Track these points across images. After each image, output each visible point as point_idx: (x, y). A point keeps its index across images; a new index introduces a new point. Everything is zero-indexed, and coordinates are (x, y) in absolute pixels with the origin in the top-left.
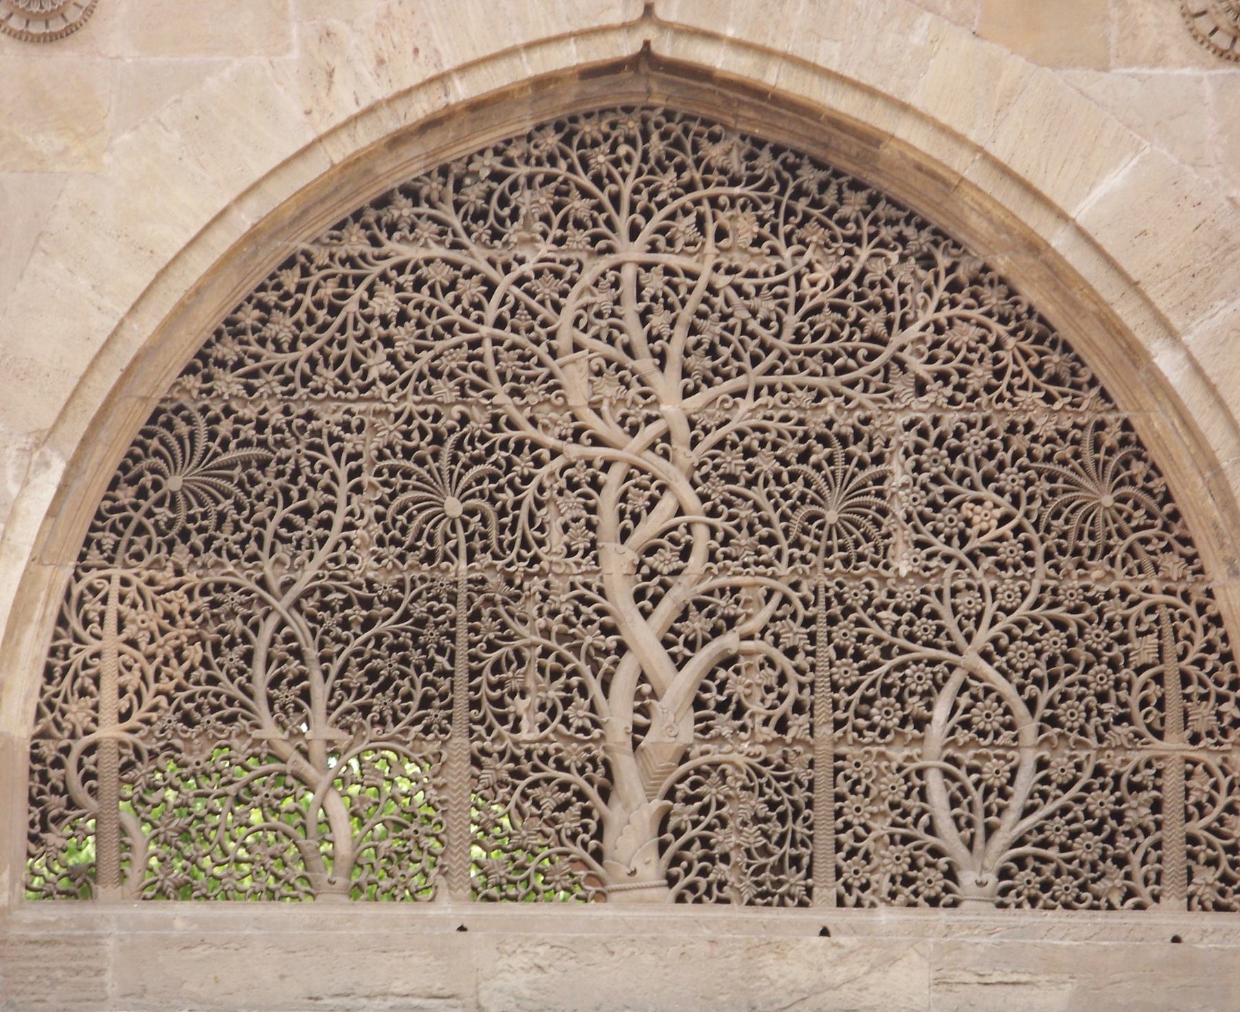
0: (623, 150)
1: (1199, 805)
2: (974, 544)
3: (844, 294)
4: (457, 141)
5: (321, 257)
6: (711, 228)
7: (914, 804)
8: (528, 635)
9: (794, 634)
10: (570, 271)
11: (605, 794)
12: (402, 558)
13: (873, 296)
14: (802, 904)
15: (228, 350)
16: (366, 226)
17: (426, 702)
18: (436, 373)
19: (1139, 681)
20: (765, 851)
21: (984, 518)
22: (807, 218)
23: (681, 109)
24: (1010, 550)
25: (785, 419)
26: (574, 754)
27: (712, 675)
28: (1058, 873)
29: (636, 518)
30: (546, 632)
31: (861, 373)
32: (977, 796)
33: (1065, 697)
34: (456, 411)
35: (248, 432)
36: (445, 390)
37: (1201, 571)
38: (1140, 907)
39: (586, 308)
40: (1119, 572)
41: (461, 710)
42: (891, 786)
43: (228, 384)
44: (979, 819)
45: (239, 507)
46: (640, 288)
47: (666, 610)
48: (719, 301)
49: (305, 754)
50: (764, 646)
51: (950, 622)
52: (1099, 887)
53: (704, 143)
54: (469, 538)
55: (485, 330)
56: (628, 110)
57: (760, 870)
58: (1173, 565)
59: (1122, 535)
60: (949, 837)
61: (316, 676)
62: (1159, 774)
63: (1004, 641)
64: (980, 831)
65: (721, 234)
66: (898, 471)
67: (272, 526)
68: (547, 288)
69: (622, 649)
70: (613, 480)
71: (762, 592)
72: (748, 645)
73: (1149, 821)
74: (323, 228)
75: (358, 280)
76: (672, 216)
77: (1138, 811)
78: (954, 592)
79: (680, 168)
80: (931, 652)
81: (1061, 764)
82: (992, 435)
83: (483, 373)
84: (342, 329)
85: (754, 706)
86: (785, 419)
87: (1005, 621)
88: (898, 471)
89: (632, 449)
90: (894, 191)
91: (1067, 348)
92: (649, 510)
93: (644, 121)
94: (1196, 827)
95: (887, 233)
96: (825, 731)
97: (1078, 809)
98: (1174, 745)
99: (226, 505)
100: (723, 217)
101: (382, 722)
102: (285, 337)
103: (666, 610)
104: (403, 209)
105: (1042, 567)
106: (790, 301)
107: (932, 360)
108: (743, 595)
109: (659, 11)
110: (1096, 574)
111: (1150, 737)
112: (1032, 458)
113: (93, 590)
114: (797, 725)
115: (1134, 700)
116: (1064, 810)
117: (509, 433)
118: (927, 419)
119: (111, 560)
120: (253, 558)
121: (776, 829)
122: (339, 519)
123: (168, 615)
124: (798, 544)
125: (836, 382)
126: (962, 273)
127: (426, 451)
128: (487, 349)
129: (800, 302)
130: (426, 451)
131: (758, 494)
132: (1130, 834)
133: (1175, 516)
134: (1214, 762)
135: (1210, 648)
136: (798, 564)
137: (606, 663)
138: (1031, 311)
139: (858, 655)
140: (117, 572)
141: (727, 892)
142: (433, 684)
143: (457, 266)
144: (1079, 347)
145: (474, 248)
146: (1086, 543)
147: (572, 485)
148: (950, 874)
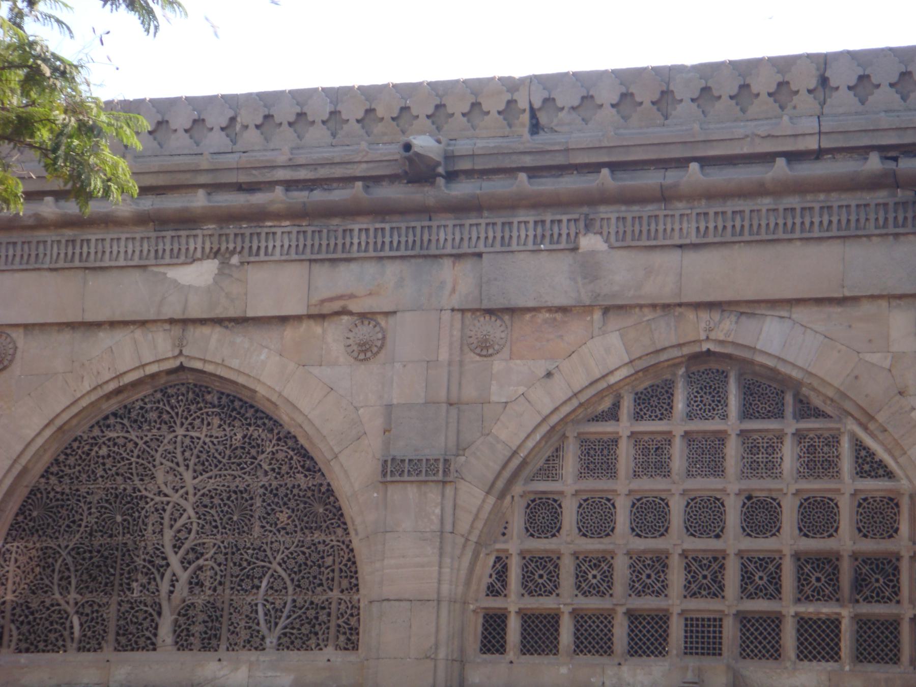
0: (180, 398)
1: (342, 614)
2: (279, 526)
3: (244, 443)
4: (128, 397)
5: (85, 437)
6: (205, 422)
7: (253, 615)
8: (139, 561)
9: (220, 558)
10: (161, 438)
11: (160, 614)
12: (102, 536)
13: (253, 443)
14: (216, 650)
15: (55, 469)
16: (100, 427)
17: (106, 584)
18: (117, 474)
19: (326, 572)
20: (206, 633)
21: (283, 517)
22: (235, 418)
23: (199, 383)
24: (290, 528)
25: (224, 486)
26: (149, 601)
27: (195, 573)
28: (296, 638)
29: (175, 520)
30: (144, 560)
31: (248, 469)
32: (272, 612)
33: (303, 578)
34: (122, 487)
35: (59, 496)
36: (119, 479)
37: (348, 534)
38: (321, 649)
39: (165, 450)
40: (323, 535)
41: (116, 587)
42: (246, 609)
43: (53, 480)
44: (273, 620)
45: (54, 521)
46: (183, 443)
47: (182, 552)
48: (206, 447)
49: (68, 603)
50: (211, 563)
51: (269, 553)
52: (307, 643)
53: (205, 394)
54: (124, 529)
55: (133, 459)
56: (183, 384)
57: (204, 639)
58: (340, 531)
59: (325, 522)
60: (263, 627)
61: (73, 576)
62: (330, 603)
63: (286, 559)
64: (273, 624)
65: (209, 424)
66: (258, 502)
67: (63, 527)
68: (154, 445)
69: (168, 565)
70: (169, 508)
71: (212, 544)
72: (206, 563)
73: (326, 620)
74: (86, 428)
75: (96, 444)
76: (194, 419)
77: (323, 617)
78: (272, 543)
79: (198, 403)
80: (263, 564)
81: (300, 601)
82: (287, 489)
83: (131, 474)
84: (90, 461)
85: (207, 584)
86: (224, 486)
87: (287, 552)
88: (258, 502)
89: (175, 498)
90: (262, 408)
91: (312, 459)
92: (180, 518)
93: (188, 388)
94: (340, 622)
95: (259, 422)
96: (228, 591)
97: (304, 617)
98: (335, 594)
99: (50, 520)
100: (209, 419)
101: (91, 592)
102: (72, 464)
103: (182, 552)
104: (112, 420)
105: (299, 534)
106: (228, 446)
107: (270, 464)
108: (206, 546)
109: (184, 352)
110: (316, 536)
111: (328, 590)
112: (299, 497)
113: (8, 550)
114: (220, 588)
115: (324, 579)
116: (300, 616)
117: (138, 494)
118: (267, 485)
119: (14, 540)
120: (57, 538)
121: (210, 625)
122: (84, 524)
123: (30, 558)
124: (225, 528)
125: (240, 473)
126: (281, 435)
127: (112, 500)
128: (134, 466)
129: (231, 445)
130: (112, 500)
131: (213, 511)
132: (320, 624)
133: (342, 515)
134: (347, 599)
135: (349, 560)
136: (225, 535)
137: (162, 570)
138: (302, 447)
139: (240, 565)
140: (15, 544)
141: (193, 647)
142: (108, 578)
143: (126, 438)
144: (316, 459)
145: (132, 432)
146: (314, 525)
147: (157, 510)
148: (263, 638)
